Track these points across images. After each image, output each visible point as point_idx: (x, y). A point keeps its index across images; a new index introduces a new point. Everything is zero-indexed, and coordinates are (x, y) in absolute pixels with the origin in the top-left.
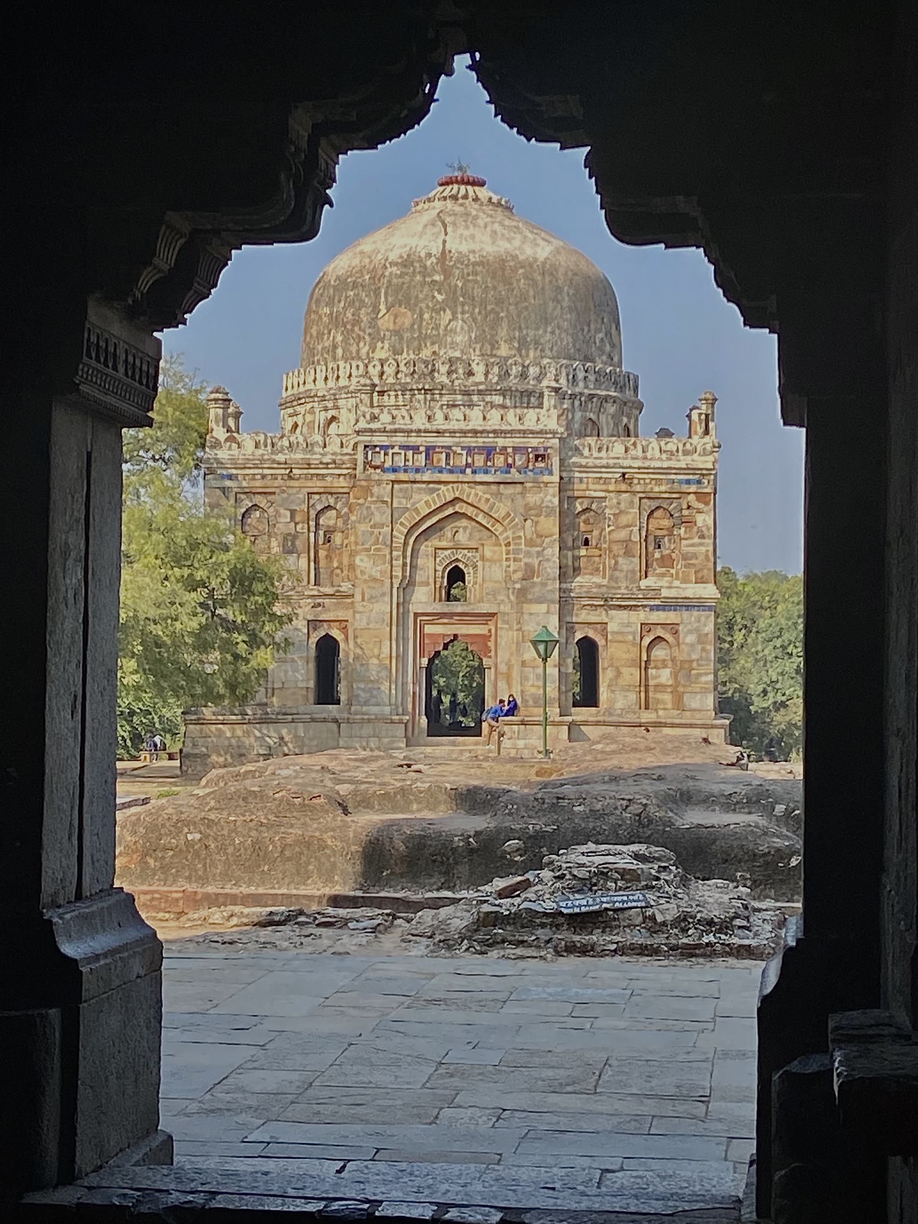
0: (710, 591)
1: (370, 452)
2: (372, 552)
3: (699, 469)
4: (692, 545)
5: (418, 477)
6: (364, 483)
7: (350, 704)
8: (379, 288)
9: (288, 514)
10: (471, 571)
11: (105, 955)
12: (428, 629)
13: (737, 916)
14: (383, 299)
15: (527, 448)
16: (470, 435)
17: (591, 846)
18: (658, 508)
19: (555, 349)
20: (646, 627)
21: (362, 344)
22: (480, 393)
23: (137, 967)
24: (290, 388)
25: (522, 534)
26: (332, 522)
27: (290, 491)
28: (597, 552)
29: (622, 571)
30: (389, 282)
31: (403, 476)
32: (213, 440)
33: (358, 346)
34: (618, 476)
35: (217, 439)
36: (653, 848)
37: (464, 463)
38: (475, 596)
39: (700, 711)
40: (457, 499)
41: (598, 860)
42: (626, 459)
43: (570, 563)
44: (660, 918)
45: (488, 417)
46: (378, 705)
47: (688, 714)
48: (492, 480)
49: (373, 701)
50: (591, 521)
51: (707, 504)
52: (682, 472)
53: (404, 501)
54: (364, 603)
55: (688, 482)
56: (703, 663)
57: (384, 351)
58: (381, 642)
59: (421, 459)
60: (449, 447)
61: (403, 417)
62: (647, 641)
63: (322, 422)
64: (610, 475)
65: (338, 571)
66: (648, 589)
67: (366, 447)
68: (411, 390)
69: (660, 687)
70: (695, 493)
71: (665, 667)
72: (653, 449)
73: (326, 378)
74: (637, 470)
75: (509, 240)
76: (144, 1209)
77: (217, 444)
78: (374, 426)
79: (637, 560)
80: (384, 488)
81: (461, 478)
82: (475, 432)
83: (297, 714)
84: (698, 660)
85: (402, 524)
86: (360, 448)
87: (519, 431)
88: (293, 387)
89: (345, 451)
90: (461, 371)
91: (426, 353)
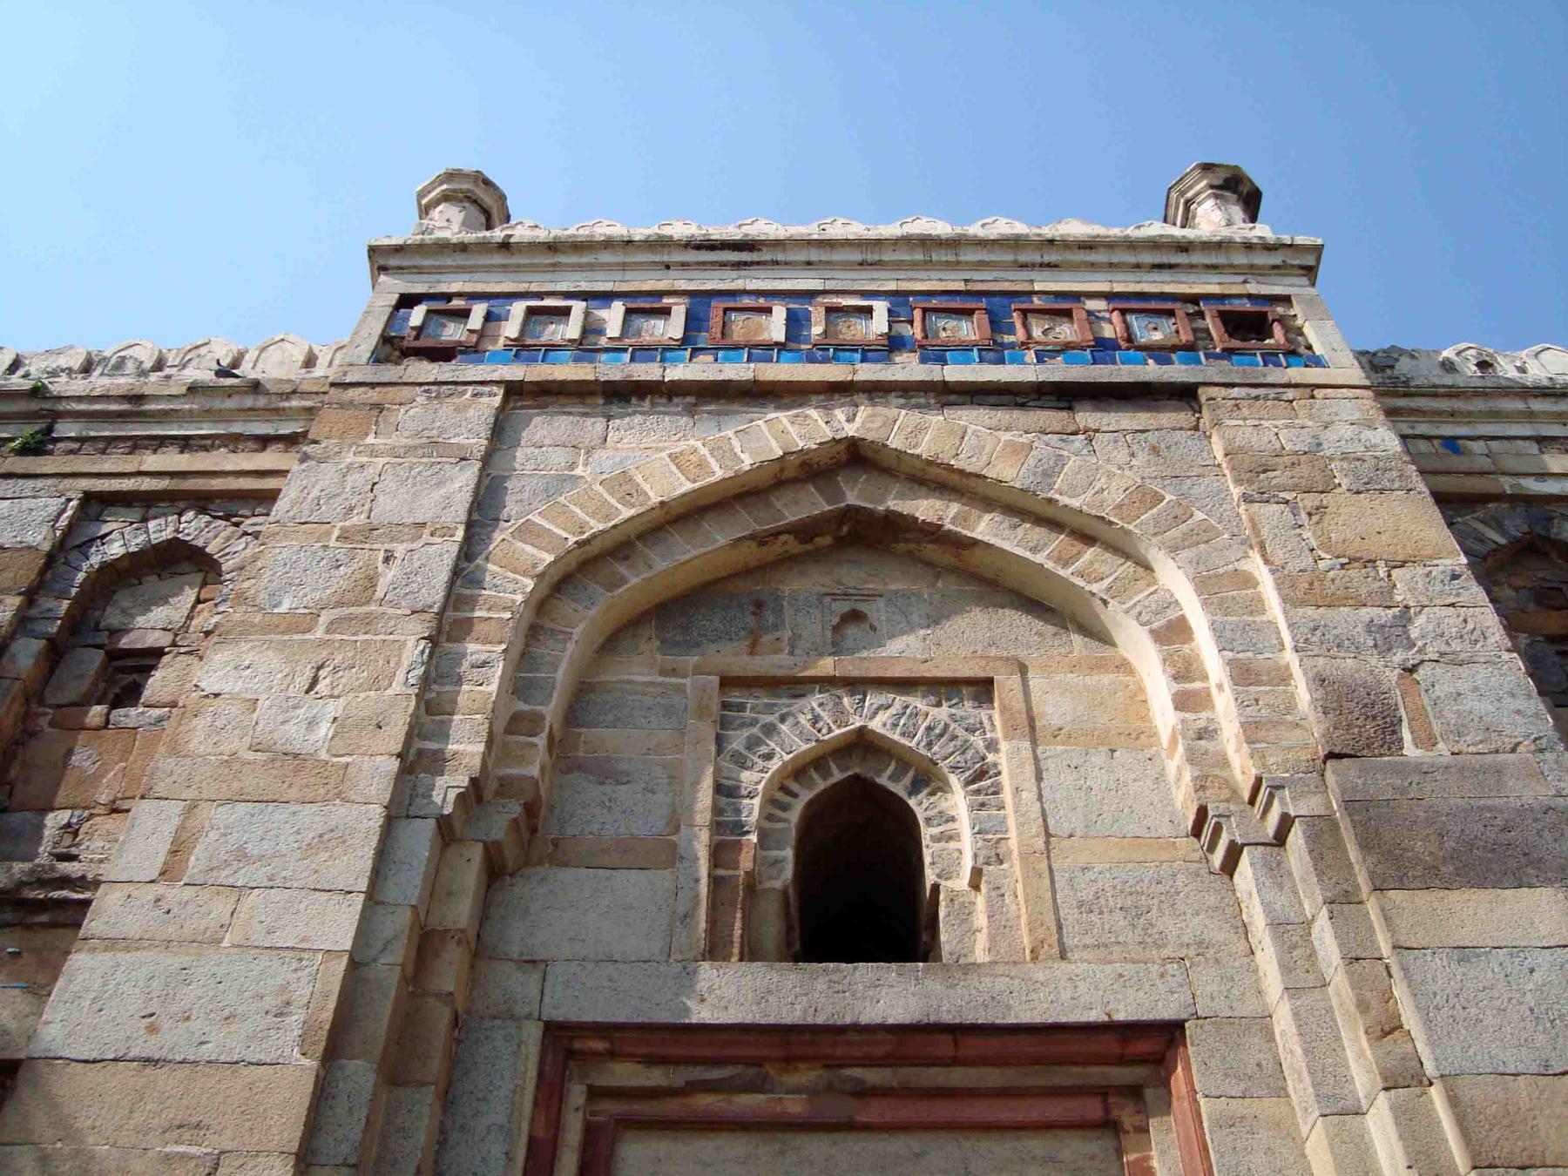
2: (319, 633)
5: (648, 372)
10: (958, 800)
31: (565, 370)
38: (1001, 926)
54: (174, 894)
85: (527, 532)
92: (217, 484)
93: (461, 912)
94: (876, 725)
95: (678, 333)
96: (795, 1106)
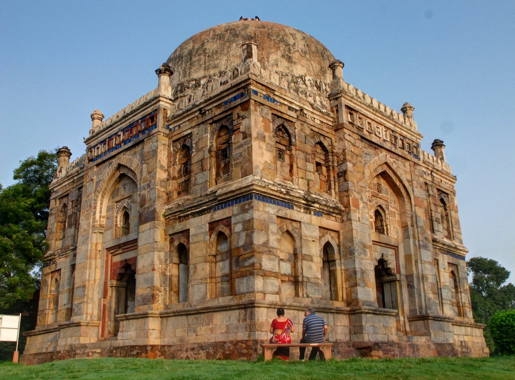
9: (71, 203)
31: (99, 161)
40: (120, 166)
52: (230, 91)
55: (235, 98)
70: (240, 104)
84: (244, 246)
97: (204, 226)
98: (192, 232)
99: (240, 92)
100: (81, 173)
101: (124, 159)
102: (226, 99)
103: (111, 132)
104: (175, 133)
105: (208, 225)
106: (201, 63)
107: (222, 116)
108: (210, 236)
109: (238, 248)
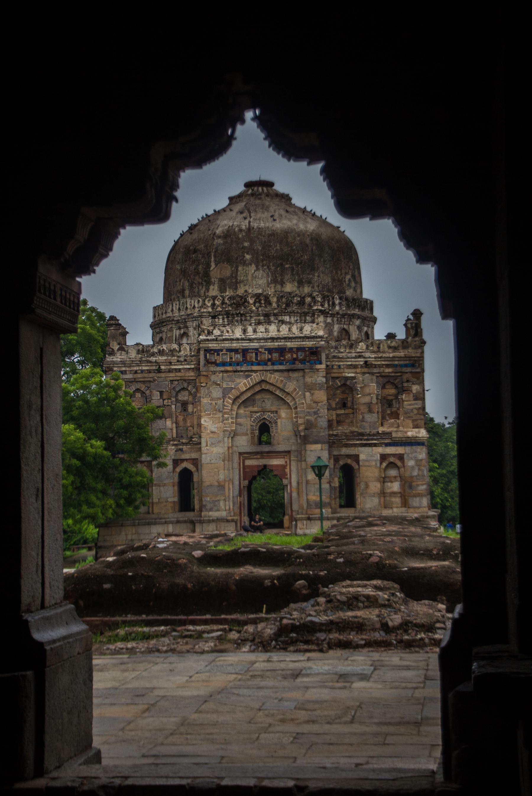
0: (423, 433)
1: (208, 354)
3: (412, 357)
4: (410, 405)
5: (239, 368)
6: (204, 373)
7: (201, 510)
8: (210, 252)
9: (158, 393)
10: (274, 425)
11: (59, 640)
12: (248, 462)
13: (438, 621)
14: (213, 259)
15: (305, 348)
16: (269, 341)
17: (348, 582)
18: (389, 382)
19: (321, 286)
20: (384, 457)
21: (200, 288)
22: (275, 315)
23: (78, 648)
24: (157, 316)
25: (304, 401)
26: (186, 398)
27: (160, 380)
28: (350, 411)
29: (367, 422)
30: (217, 248)
32: (111, 350)
33: (198, 288)
34: (362, 363)
35: (113, 349)
36: (386, 582)
37: (267, 358)
39: (418, 508)
41: (351, 589)
42: (367, 352)
43: (335, 419)
44: (390, 624)
45: (281, 329)
46: (218, 510)
47: (411, 510)
48: (284, 368)
49: (216, 508)
50: (347, 392)
51: (418, 378)
53: (230, 383)
54: (208, 448)
55: (406, 366)
56: (418, 477)
57: (215, 291)
58: (219, 471)
59: (239, 357)
60: (257, 349)
61: (228, 332)
62: (384, 465)
63: (177, 336)
64: (357, 363)
65: (191, 428)
66: (384, 433)
67: (205, 350)
68: (233, 314)
69: (394, 494)
70: (411, 372)
71: (396, 481)
72: (383, 345)
73: (179, 309)
74: (374, 359)
75: (290, 220)
76: (86, 788)
77: (112, 353)
78: (209, 338)
79: (375, 415)
80: (218, 376)
81: (266, 368)
82: (273, 339)
83: (169, 518)
84: (416, 476)
85: (229, 398)
86: (202, 353)
87: (300, 338)
88: (159, 315)
89: (193, 354)
90: (263, 302)
91: (241, 291)
92: (186, 378)
93: (230, 445)
94: (266, 417)
95: (241, 360)
96: (259, 457)
97: (375, 456)
98: (362, 457)
99: (411, 362)
100: (175, 365)
101: (274, 378)
102: (396, 363)
103: (247, 344)
104: (334, 371)
105: (379, 455)
106: (294, 273)
107: (390, 375)
108: (381, 463)
109: (412, 477)
